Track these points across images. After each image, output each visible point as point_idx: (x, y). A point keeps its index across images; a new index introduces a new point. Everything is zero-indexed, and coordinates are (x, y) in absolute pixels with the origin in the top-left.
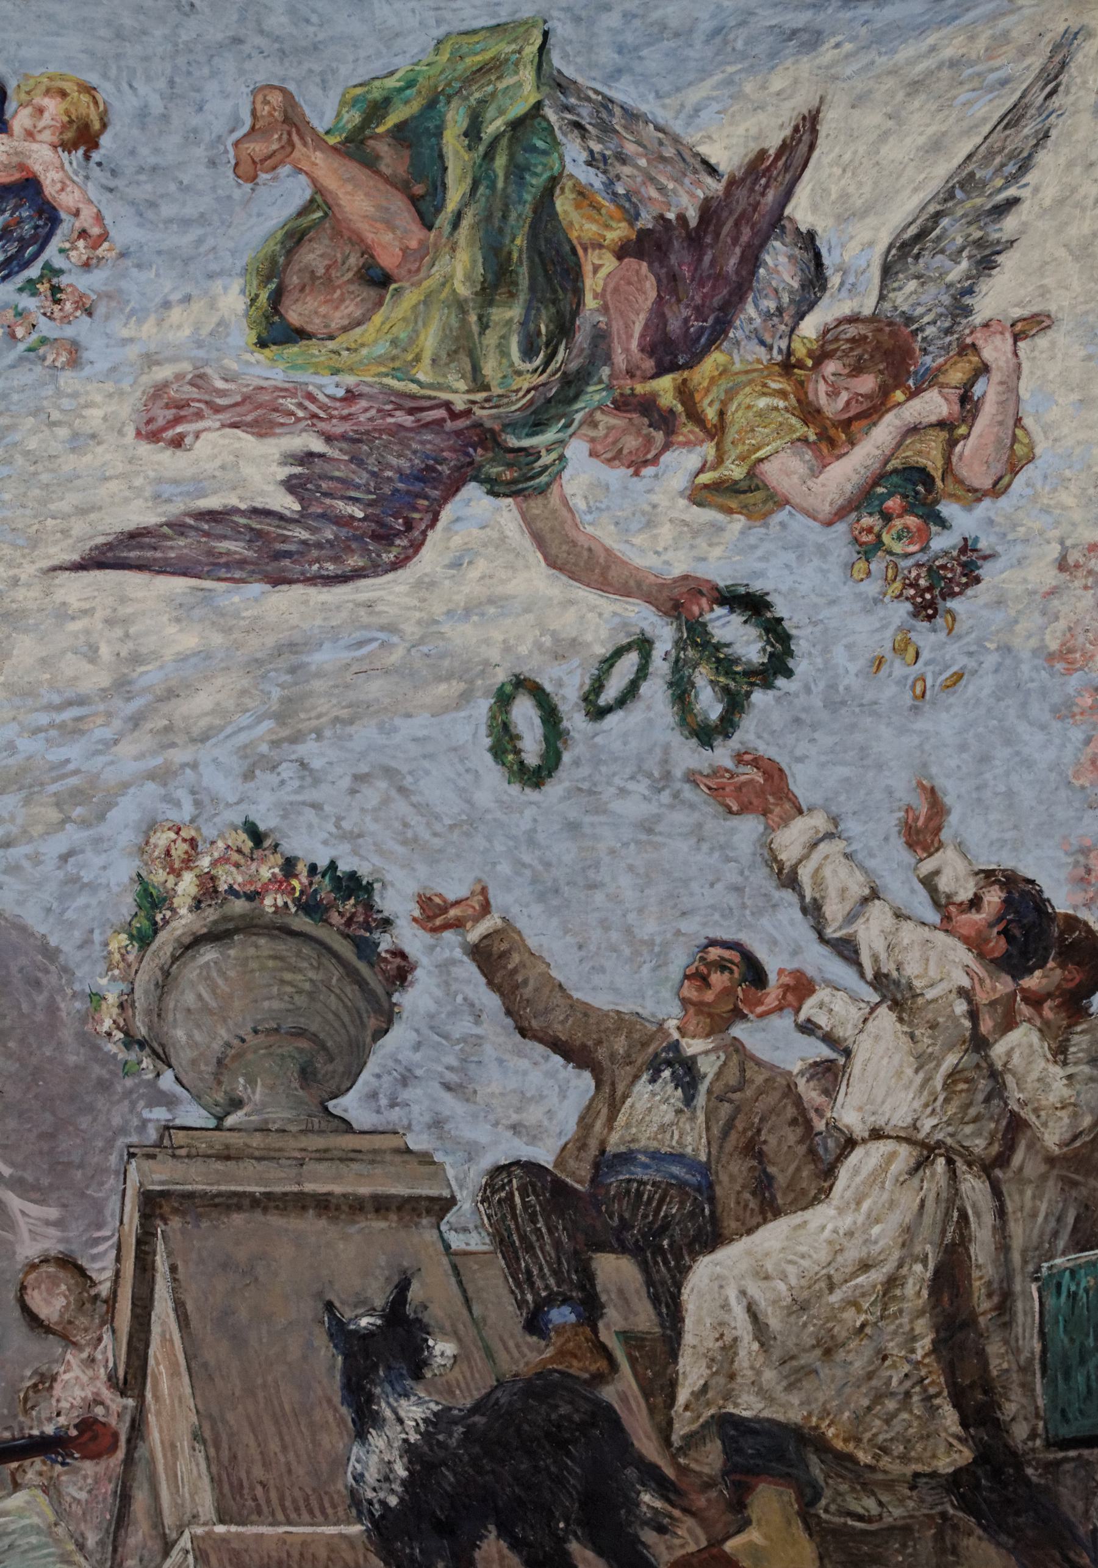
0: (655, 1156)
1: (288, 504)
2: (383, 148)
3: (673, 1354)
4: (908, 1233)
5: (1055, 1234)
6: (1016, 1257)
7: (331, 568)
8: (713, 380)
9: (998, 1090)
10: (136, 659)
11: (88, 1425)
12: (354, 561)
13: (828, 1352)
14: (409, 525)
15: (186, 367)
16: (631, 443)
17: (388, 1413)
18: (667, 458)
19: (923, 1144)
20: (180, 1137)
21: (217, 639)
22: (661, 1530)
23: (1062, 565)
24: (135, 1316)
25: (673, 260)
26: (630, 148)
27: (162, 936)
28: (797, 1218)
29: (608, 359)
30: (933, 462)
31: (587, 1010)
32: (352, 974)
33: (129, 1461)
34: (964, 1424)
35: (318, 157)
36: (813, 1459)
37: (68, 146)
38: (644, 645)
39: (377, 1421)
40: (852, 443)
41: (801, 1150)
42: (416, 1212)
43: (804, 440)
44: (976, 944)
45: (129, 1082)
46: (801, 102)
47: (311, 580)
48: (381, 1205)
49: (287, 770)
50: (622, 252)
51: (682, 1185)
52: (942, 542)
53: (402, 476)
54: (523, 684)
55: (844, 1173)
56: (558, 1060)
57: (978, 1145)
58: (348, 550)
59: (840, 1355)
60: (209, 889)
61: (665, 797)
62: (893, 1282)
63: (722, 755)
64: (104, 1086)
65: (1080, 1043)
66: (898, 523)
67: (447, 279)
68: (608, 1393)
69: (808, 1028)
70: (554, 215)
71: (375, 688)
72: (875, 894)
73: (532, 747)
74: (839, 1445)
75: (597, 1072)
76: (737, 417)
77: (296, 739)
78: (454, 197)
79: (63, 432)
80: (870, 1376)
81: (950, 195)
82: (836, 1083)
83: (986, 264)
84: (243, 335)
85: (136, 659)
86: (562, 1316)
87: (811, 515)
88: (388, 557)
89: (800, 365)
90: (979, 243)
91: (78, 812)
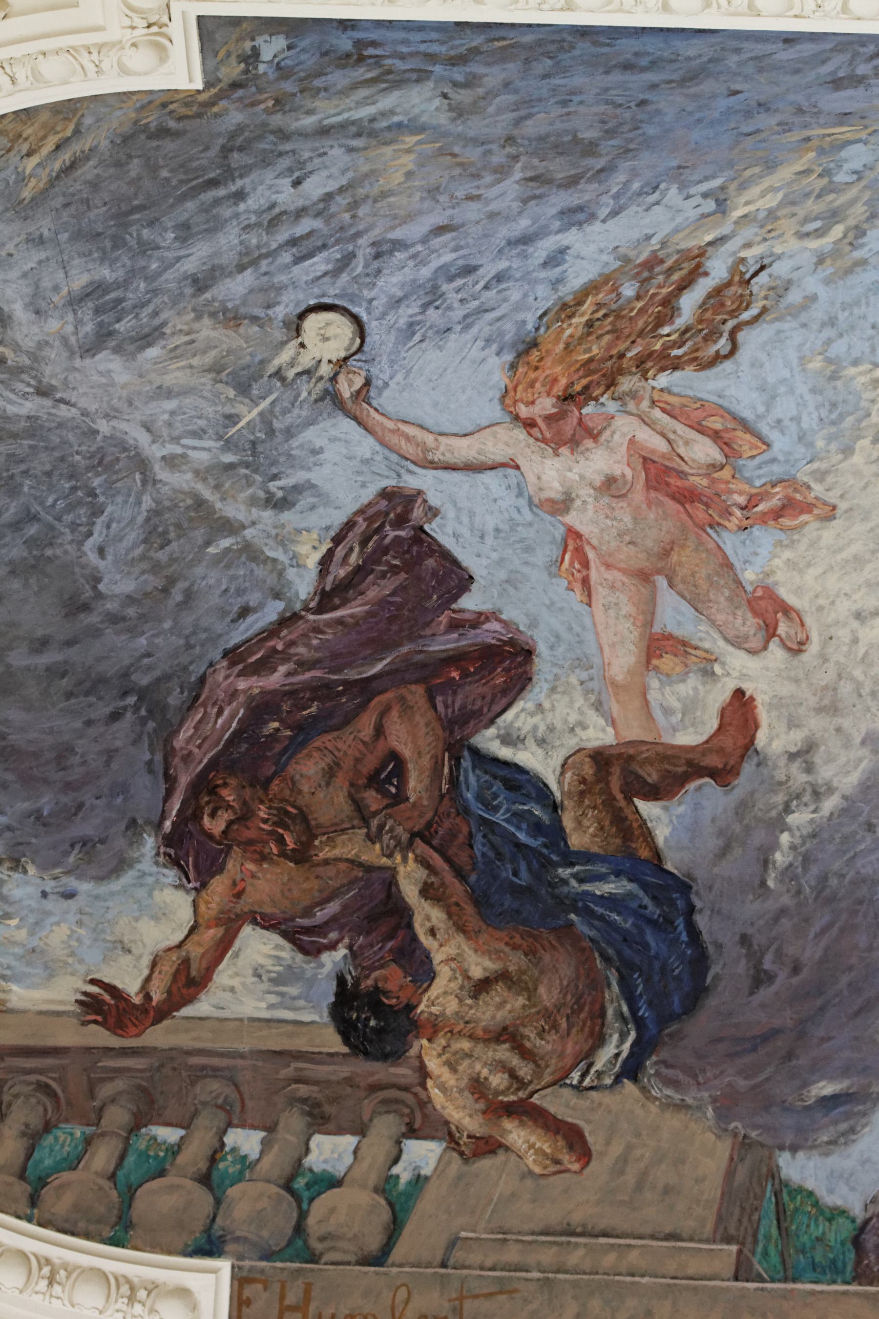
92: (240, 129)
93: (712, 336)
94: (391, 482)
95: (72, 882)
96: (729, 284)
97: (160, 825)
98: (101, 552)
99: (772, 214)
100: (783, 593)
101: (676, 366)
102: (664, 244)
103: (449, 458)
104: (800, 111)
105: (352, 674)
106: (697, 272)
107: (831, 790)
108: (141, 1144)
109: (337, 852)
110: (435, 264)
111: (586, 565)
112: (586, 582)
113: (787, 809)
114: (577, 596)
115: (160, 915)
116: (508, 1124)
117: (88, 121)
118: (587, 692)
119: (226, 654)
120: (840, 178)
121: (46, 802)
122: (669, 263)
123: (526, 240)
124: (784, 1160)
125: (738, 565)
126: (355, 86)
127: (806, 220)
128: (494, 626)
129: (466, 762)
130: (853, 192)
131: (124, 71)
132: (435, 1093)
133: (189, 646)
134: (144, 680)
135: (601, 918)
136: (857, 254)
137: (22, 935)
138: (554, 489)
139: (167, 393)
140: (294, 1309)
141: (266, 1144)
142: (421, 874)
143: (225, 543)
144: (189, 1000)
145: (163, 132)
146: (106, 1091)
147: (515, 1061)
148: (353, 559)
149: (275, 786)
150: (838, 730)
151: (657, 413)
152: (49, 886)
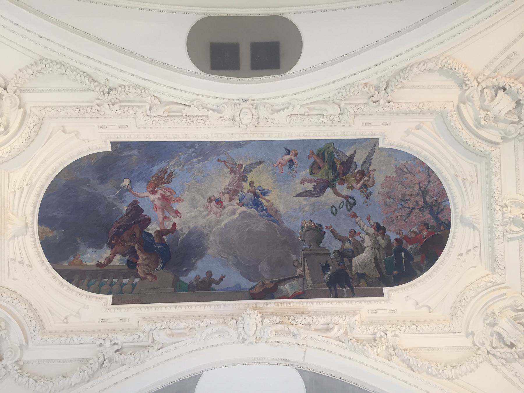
1: (313, 190)
4: (371, 255)
7: (317, 196)
11: (300, 275)
12: (319, 195)
13: (366, 266)
16: (341, 183)
21: (307, 203)
22: (353, 283)
23: (378, 193)
33: (304, 278)
35: (315, 156)
38: (343, 202)
39: (326, 274)
46: (354, 150)
47: (315, 197)
48: (324, 254)
49: (314, 215)
50: (340, 164)
52: (368, 191)
54: (333, 206)
57: (377, 247)
62: (371, 260)
63: (351, 212)
65: (385, 237)
68: (346, 271)
69: (360, 237)
71: (321, 207)
72: (365, 225)
73: (334, 212)
77: (314, 212)
78: (326, 161)
83: (370, 165)
84: (309, 173)
86: (341, 264)
88: (321, 194)
93: (169, 180)
95: (96, 250)
99: (174, 164)
100: (179, 211)
103: (141, 196)
106: (167, 172)
108: (102, 281)
112: (156, 210)
114: (156, 212)
115: (106, 253)
116: (147, 276)
118: (157, 224)
125: (173, 207)
128: (147, 216)
129: (143, 233)
136: (184, 169)
142: (138, 246)
143: (115, 208)
144: (110, 263)
147: (148, 268)
150: (185, 227)
151: (163, 190)
152: (93, 250)
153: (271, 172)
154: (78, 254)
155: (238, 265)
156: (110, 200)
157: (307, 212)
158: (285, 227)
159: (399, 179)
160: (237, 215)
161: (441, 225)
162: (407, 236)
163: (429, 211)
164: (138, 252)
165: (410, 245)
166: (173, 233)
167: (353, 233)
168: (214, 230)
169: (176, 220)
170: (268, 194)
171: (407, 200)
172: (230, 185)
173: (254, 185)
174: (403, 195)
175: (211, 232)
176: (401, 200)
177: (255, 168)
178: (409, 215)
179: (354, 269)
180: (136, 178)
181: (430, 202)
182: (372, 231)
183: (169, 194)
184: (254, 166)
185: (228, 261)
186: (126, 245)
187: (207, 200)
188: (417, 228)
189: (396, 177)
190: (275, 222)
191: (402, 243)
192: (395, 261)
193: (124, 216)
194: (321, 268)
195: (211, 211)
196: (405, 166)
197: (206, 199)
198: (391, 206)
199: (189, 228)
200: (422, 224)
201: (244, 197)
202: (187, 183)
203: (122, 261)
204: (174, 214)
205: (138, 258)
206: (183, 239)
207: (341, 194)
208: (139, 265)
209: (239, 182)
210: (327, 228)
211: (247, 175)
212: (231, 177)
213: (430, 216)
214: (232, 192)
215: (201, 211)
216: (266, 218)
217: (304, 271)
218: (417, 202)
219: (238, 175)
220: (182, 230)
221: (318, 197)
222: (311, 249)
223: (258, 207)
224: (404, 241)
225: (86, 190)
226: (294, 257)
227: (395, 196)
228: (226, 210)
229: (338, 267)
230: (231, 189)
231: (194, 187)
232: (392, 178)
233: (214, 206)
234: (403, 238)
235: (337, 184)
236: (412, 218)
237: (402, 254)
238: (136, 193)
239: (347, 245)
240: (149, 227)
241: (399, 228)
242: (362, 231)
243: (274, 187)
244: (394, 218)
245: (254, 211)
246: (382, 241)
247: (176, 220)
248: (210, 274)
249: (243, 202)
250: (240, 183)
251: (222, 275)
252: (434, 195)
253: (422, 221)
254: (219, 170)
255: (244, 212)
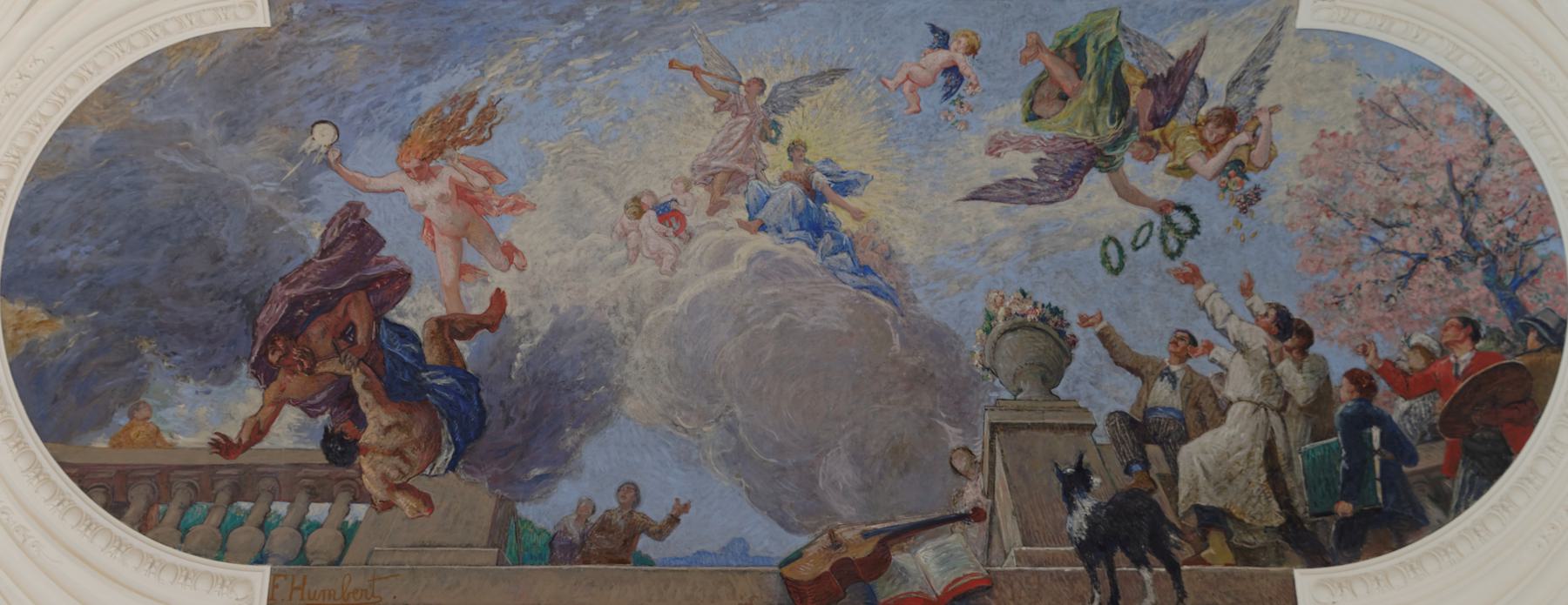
0: (1164, 408)
2: (1067, 52)
3: (1176, 482)
4: (1254, 436)
5: (1305, 436)
6: (1292, 444)
7: (1048, 199)
8: (1172, 130)
9: (1280, 384)
10: (984, 232)
12: (1056, 196)
13: (1230, 481)
14: (1073, 183)
15: (1001, 129)
16: (1145, 153)
17: (1079, 505)
18: (1157, 157)
19: (1256, 403)
20: (1002, 403)
21: (1011, 225)
23: (1288, 193)
24: (990, 469)
25: (1159, 89)
26: (1146, 51)
27: (994, 330)
28: (1215, 431)
29: (1138, 124)
30: (1244, 158)
31: (1137, 355)
32: (1057, 343)
34: (1281, 507)
36: (1229, 522)
37: (968, 54)
38: (1151, 224)
40: (1217, 152)
41: (1214, 405)
42: (1084, 430)
43: (1202, 151)
44: (1267, 329)
45: (985, 383)
47: (1041, 203)
48: (1071, 427)
49: (1034, 270)
50: (1143, 87)
51: (1174, 418)
52: (1248, 186)
53: (1072, 167)
55: (1229, 414)
56: (1129, 373)
57: (1275, 403)
58: (1053, 192)
59: (1235, 482)
60: (1009, 314)
61: (1160, 278)
62: (1250, 455)
63: (1177, 263)
64: (976, 384)
65: (1306, 365)
66: (1233, 180)
67: (1087, 97)
69: (1213, 361)
70: (1121, 75)
72: (1232, 313)
74: (1237, 516)
75: (1142, 377)
76: (1180, 143)
77: (1037, 259)
79: (962, 152)
80: (1246, 490)
81: (1248, 65)
82: (1224, 381)
83: (1260, 88)
84: (1020, 117)
85: (984, 232)
86: (1136, 468)
87: (1205, 177)
88: (1067, 194)
89: (1200, 125)
90: (1257, 81)
91: (965, 287)
92: (286, 45)
93: (480, 131)
94: (351, 199)
95: (209, 387)
96: (487, 107)
97: (249, 359)
98: (228, 233)
100: (515, 244)
101: (468, 144)
102: (460, 90)
103: (377, 188)
104: (511, 31)
105: (335, 287)
107: (538, 333)
109: (326, 369)
110: (368, 101)
111: (433, 235)
112: (433, 242)
113: (520, 342)
114: (430, 247)
117: (224, 41)
118: (434, 292)
119: (281, 279)
120: (529, 60)
121: (200, 350)
122: (463, 98)
123: (405, 90)
124: (519, 506)
125: (496, 232)
126: (331, 25)
127: (517, 78)
129: (383, 326)
130: (535, 65)
131: (237, 18)
132: (366, 480)
133: (265, 276)
134: (245, 292)
135: (440, 396)
136: (538, 93)
137: (186, 412)
138: (419, 201)
139: (257, 161)
140: (298, 588)
141: (289, 508)
142: (363, 378)
143: (281, 229)
144: (258, 441)
145: (255, 46)
146: (219, 485)
147: (402, 464)
148: (336, 234)
149: (300, 339)
150: (541, 305)
151: (461, 166)
152: (199, 388)
153: (874, 108)
154: (144, 402)
155: (737, 459)
156: (261, 201)
157: (1006, 260)
158: (923, 317)
159: (1369, 145)
160: (737, 268)
161: (1526, 329)
162: (1394, 364)
163: (1484, 270)
164: (365, 398)
165: (1407, 398)
166: (492, 328)
167: (1186, 344)
168: (648, 321)
169: (504, 280)
170: (858, 190)
171: (1399, 225)
172: (713, 152)
173: (807, 156)
174: (1385, 204)
175: (637, 327)
176: (1376, 221)
177: (812, 93)
178: (1405, 279)
179: (1183, 489)
180: (358, 122)
181: (1488, 237)
182: (1258, 338)
183: (479, 181)
184: (806, 87)
185: (699, 447)
186: (321, 368)
187: (626, 208)
188: (1433, 336)
189: (1359, 134)
190: (885, 297)
191: (1373, 388)
192: (1343, 462)
193: (311, 261)
194: (1056, 484)
195: (638, 249)
196: (1397, 97)
197: (623, 201)
198: (1334, 245)
199: (555, 309)
200: (1455, 321)
201: (768, 198)
202: (551, 145)
203: (304, 435)
204: (500, 258)
205: (360, 420)
206: (533, 353)
207: (1144, 196)
208: (365, 450)
209: (750, 140)
210: (1084, 321)
211: (780, 119)
212: (718, 125)
213: (1485, 290)
214: (719, 178)
215: (599, 249)
216: (848, 278)
217: (990, 492)
218: (1436, 234)
219: (745, 118)
220: (526, 316)
221: (1051, 202)
222: (1021, 404)
223: (820, 235)
224: (1382, 384)
225: (174, 164)
226: (953, 436)
227: (1351, 207)
228: (695, 246)
229: (1124, 482)
230: (716, 168)
231: (577, 157)
232: (1346, 138)
233: (650, 231)
234: (1378, 371)
235: (1128, 156)
236: (1416, 294)
237: (1371, 436)
238: (357, 175)
239: (1163, 394)
240: (405, 303)
241: (1365, 330)
242: (1221, 340)
243: (885, 164)
244: (1345, 290)
245: (804, 252)
246: (1298, 382)
247: (504, 280)
248: (631, 493)
249: (761, 215)
250: (753, 146)
251: (677, 500)
252: (1504, 214)
253: (1454, 310)
254: (675, 99)
255: (764, 254)
